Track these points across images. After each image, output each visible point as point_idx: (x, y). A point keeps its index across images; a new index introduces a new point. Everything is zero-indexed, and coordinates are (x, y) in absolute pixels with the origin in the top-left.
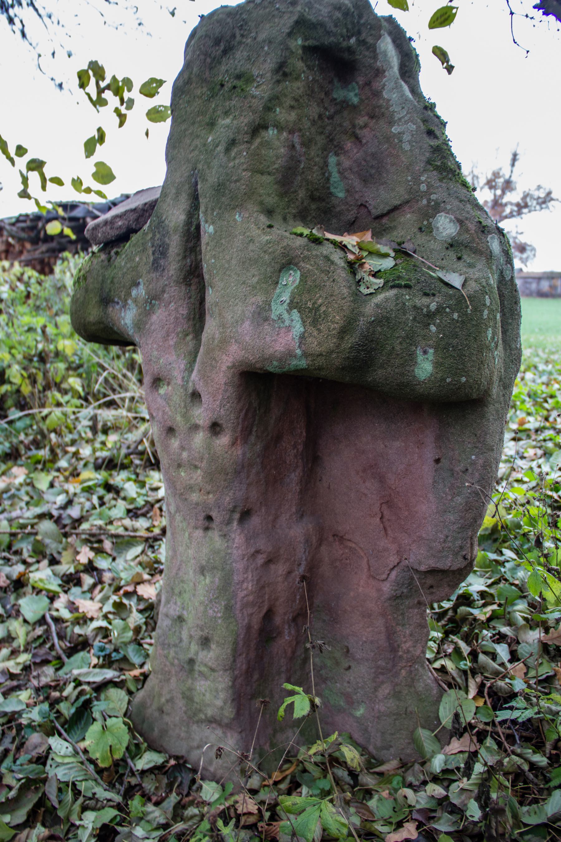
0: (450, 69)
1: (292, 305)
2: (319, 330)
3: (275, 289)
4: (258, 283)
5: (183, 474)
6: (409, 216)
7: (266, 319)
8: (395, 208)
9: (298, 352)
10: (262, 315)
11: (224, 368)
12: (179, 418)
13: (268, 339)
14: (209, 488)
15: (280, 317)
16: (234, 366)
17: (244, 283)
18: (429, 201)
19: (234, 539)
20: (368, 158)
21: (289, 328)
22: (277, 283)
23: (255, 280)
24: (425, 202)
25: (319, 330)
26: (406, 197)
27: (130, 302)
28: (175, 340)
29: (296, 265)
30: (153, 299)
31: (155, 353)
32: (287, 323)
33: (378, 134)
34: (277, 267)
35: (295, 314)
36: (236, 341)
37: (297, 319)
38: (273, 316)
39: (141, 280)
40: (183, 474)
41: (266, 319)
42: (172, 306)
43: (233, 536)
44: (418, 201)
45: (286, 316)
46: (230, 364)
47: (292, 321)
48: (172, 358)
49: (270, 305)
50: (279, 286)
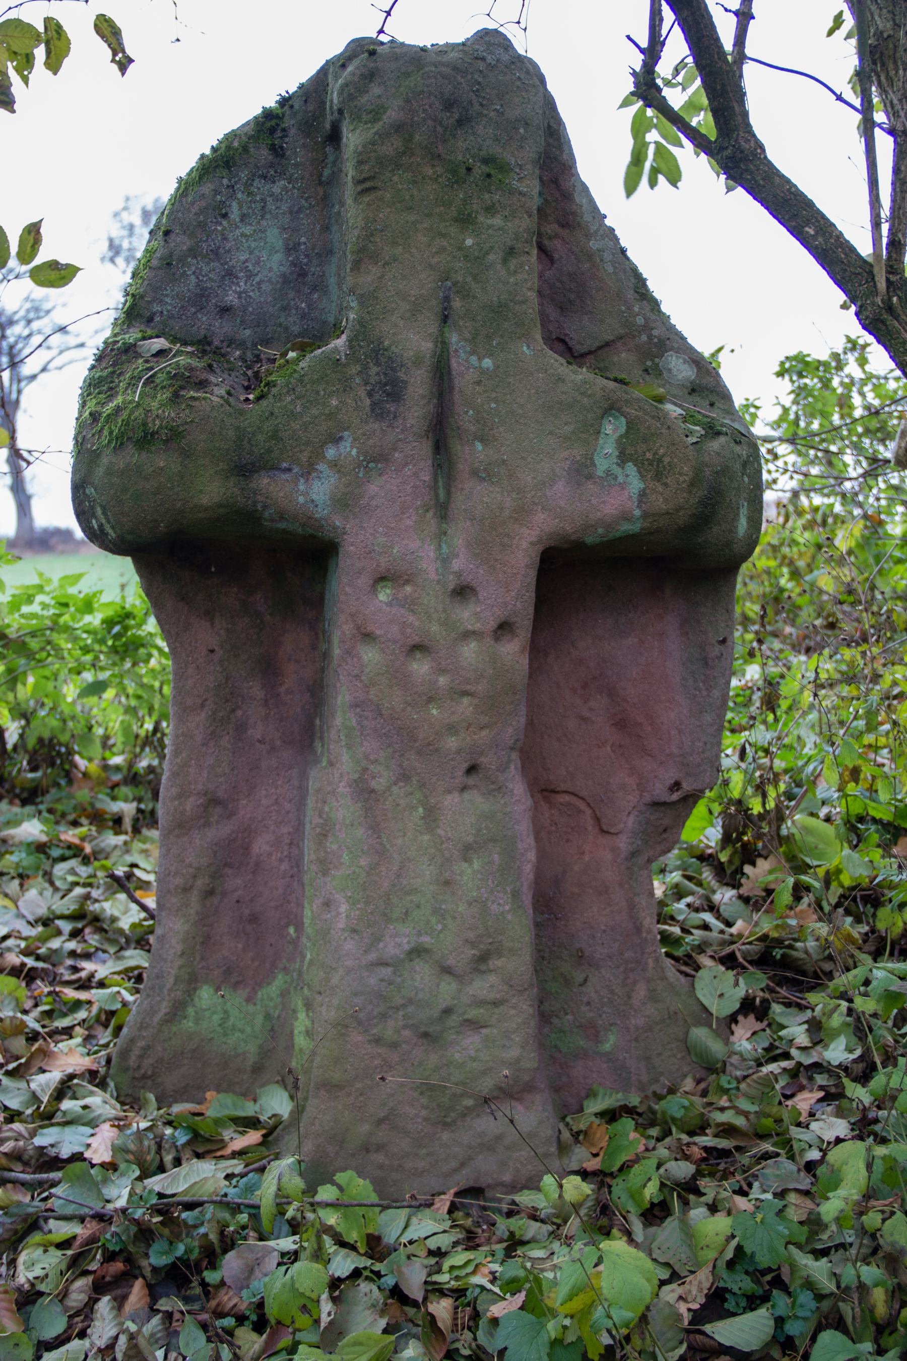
0: (124, 64)
1: (623, 458)
2: (666, 485)
3: (597, 439)
4: (573, 432)
5: (434, 712)
6: (624, 355)
7: (590, 477)
8: (607, 344)
9: (637, 513)
10: (582, 471)
11: (525, 545)
12: (435, 628)
13: (594, 501)
14: (484, 720)
15: (608, 472)
16: (540, 541)
17: (551, 433)
18: (650, 337)
19: (512, 791)
20: (565, 279)
21: (623, 486)
22: (599, 433)
23: (568, 429)
24: (644, 338)
25: (666, 485)
26: (622, 331)
27: (321, 467)
28: (413, 518)
29: (619, 410)
30: (376, 459)
31: (382, 540)
32: (621, 479)
33: (574, 249)
34: (599, 412)
35: (631, 468)
36: (543, 508)
37: (634, 474)
38: (600, 472)
39: (346, 433)
40: (434, 712)
41: (590, 477)
42: (409, 470)
43: (510, 786)
44: (634, 337)
45: (617, 470)
46: (534, 539)
47: (627, 476)
48: (414, 544)
49: (592, 459)
50: (602, 436)
